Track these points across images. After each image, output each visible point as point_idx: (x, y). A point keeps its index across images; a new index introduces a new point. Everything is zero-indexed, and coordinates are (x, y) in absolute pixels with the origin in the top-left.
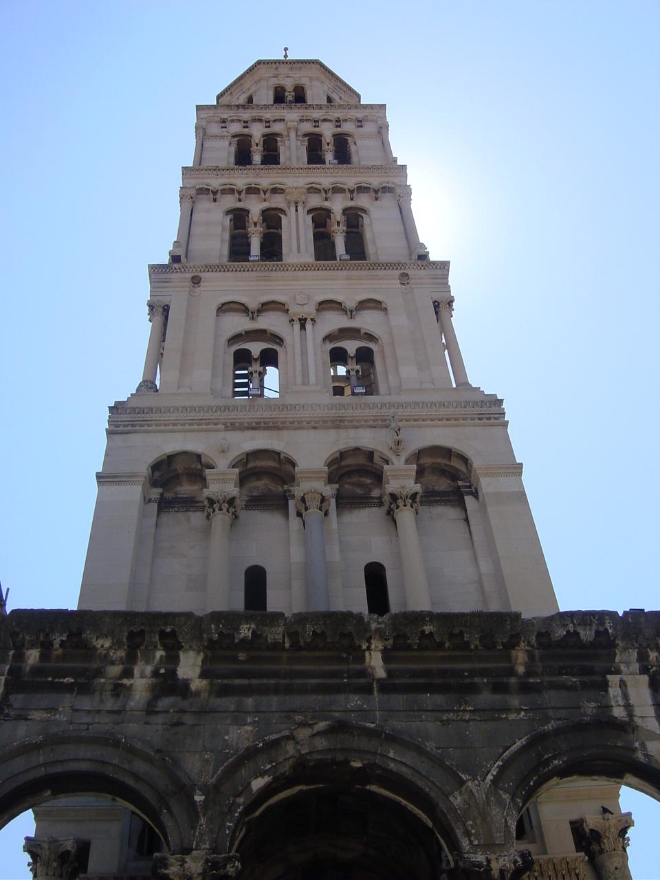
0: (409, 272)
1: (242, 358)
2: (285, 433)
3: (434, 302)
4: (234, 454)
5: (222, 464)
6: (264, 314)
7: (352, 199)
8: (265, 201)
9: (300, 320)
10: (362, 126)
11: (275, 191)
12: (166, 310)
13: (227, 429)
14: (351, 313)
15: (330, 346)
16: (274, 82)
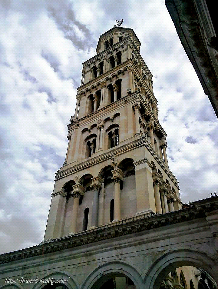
0: (127, 99)
1: (89, 144)
2: (91, 168)
3: (132, 107)
4: (80, 178)
5: (77, 183)
6: (93, 129)
7: (117, 78)
8: (96, 89)
9: (99, 128)
10: (123, 47)
11: (99, 85)
12: (71, 137)
13: (78, 171)
14: (112, 121)
15: (108, 132)
16: (105, 41)
